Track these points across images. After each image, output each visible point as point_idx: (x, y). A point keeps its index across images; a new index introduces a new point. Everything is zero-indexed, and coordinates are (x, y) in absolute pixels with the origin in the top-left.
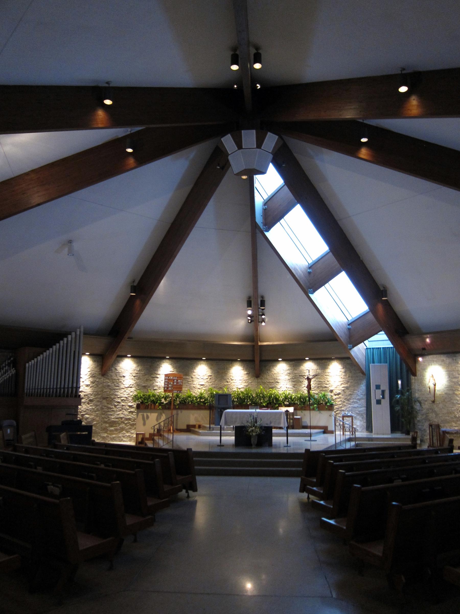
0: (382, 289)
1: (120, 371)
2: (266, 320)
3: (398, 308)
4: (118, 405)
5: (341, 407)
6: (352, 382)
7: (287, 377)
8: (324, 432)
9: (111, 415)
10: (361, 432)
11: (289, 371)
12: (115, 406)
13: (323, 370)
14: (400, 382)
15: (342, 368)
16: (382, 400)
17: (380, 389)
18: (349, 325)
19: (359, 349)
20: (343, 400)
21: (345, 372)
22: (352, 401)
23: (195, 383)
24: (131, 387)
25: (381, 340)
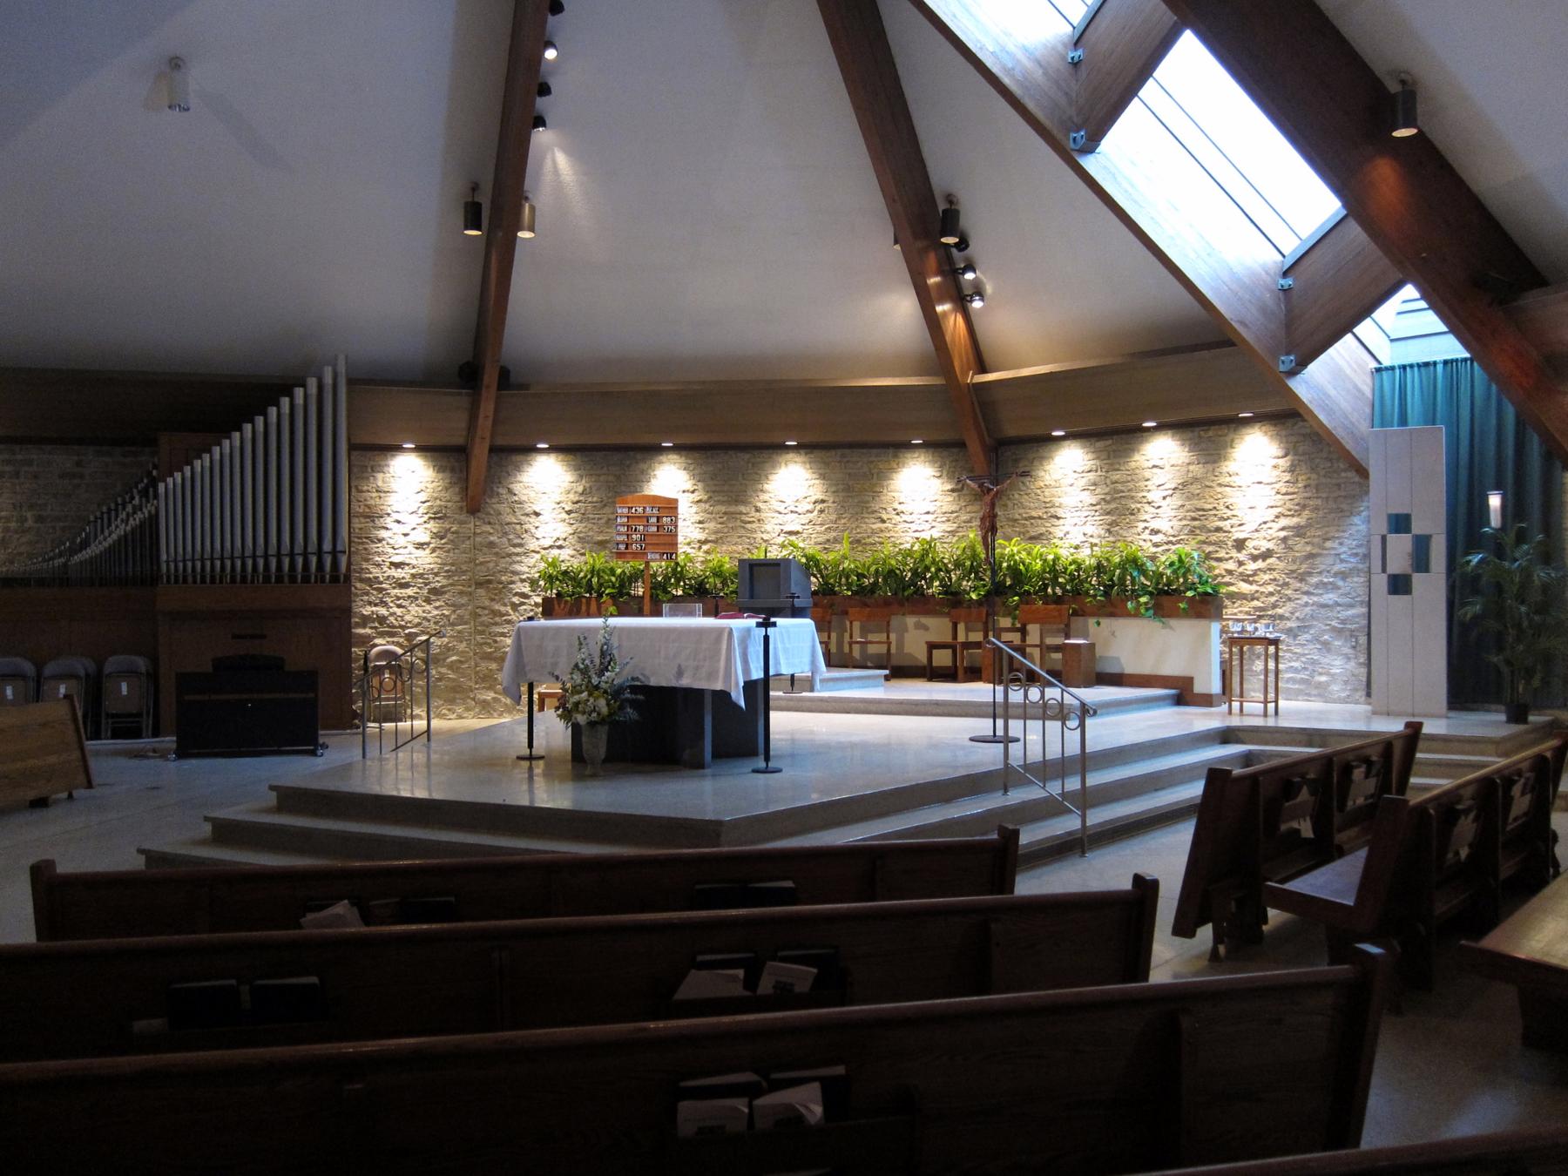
0: (1393, 87)
1: (524, 498)
2: (989, 289)
3: (1488, 176)
4: (523, 604)
5: (1274, 606)
6: (1316, 509)
7: (1088, 498)
8: (1180, 700)
9: (503, 635)
10: (1344, 701)
11: (1092, 476)
12: (515, 607)
13: (1210, 467)
14: (1495, 501)
15: (1280, 453)
16: (1417, 578)
17: (1407, 530)
18: (1285, 274)
19: (1338, 374)
20: (1282, 578)
21: (1292, 469)
22: (1314, 580)
23: (768, 527)
24: (560, 547)
25: (1406, 330)
